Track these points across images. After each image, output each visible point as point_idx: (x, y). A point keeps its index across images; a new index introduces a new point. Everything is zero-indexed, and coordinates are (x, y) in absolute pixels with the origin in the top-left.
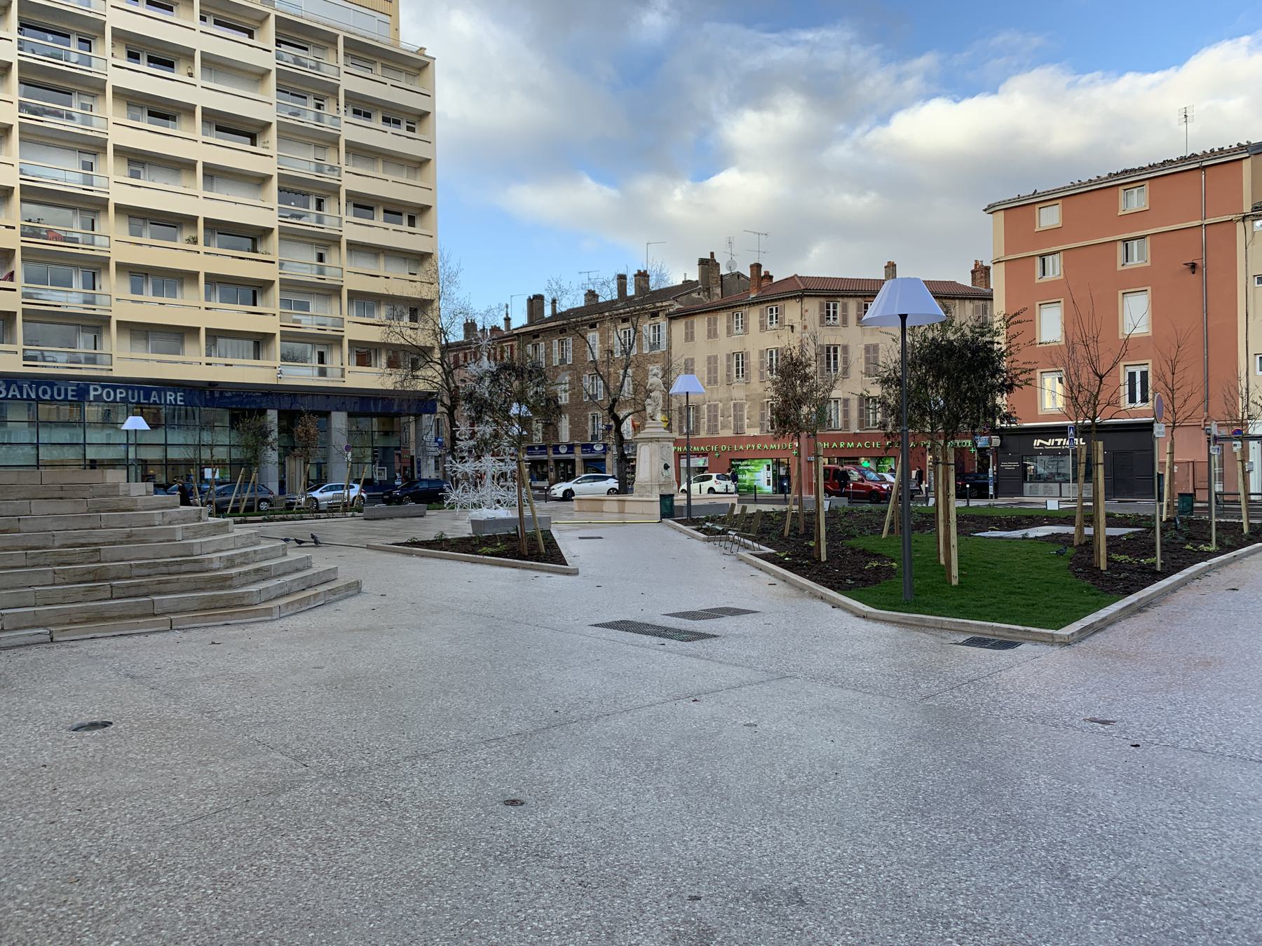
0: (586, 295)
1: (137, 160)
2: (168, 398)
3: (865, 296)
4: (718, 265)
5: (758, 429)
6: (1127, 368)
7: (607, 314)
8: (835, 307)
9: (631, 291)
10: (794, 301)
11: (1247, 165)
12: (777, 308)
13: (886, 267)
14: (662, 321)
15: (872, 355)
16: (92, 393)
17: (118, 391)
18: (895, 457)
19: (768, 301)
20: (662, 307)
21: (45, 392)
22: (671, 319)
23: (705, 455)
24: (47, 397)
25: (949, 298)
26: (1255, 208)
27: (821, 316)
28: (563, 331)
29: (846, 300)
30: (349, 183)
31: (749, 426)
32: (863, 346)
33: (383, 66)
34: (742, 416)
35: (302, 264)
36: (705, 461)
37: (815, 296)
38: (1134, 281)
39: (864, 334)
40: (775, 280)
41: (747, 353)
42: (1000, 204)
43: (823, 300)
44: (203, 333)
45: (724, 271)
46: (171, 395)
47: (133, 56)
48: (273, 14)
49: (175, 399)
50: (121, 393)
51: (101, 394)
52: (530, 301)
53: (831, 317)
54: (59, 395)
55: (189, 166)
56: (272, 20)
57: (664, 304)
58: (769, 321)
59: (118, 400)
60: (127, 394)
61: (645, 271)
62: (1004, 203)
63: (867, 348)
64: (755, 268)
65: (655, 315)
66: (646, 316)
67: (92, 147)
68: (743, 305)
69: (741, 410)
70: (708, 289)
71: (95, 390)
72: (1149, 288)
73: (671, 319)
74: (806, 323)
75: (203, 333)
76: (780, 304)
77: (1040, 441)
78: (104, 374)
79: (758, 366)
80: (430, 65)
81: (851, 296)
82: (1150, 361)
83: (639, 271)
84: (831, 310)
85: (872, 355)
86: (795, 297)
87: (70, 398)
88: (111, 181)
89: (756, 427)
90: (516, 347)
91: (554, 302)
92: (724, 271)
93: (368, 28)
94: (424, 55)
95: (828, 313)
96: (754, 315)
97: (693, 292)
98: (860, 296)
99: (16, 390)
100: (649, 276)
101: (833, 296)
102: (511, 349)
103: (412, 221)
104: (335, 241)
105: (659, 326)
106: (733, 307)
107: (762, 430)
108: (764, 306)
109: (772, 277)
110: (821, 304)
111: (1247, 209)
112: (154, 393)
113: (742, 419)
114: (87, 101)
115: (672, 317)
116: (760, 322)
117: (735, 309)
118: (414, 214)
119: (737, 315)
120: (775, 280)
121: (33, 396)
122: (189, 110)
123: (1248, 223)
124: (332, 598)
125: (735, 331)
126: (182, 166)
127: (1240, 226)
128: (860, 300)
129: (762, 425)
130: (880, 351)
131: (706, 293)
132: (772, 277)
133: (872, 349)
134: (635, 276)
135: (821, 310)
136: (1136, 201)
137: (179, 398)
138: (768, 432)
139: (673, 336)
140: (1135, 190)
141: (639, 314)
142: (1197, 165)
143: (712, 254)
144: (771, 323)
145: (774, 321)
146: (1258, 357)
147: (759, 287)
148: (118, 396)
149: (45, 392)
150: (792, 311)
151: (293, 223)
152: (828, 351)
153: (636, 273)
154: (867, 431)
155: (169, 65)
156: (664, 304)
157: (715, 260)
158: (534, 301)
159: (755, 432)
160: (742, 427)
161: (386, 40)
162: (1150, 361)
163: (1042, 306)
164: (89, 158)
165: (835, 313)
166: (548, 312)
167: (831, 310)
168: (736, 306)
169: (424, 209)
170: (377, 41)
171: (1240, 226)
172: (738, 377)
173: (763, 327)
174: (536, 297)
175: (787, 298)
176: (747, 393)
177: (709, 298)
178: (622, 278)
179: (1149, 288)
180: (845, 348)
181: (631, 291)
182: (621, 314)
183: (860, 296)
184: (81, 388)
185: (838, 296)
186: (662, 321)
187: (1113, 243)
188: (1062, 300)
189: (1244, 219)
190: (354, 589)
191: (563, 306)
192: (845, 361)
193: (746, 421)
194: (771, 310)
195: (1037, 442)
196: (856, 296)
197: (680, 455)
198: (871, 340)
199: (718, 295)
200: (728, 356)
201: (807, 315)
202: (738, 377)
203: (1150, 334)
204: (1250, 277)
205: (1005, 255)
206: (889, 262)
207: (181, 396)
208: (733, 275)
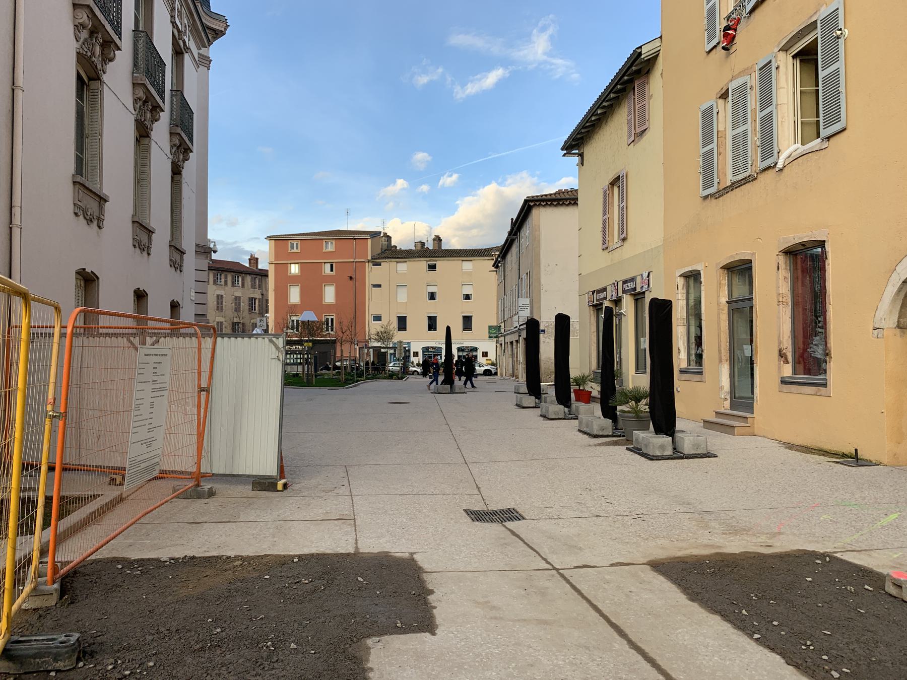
11: (369, 241)
38: (329, 280)
82: (334, 314)
111: (369, 258)
136: (330, 247)
140: (330, 242)
142: (352, 238)
162: (334, 314)
171: (367, 263)
203: (335, 303)
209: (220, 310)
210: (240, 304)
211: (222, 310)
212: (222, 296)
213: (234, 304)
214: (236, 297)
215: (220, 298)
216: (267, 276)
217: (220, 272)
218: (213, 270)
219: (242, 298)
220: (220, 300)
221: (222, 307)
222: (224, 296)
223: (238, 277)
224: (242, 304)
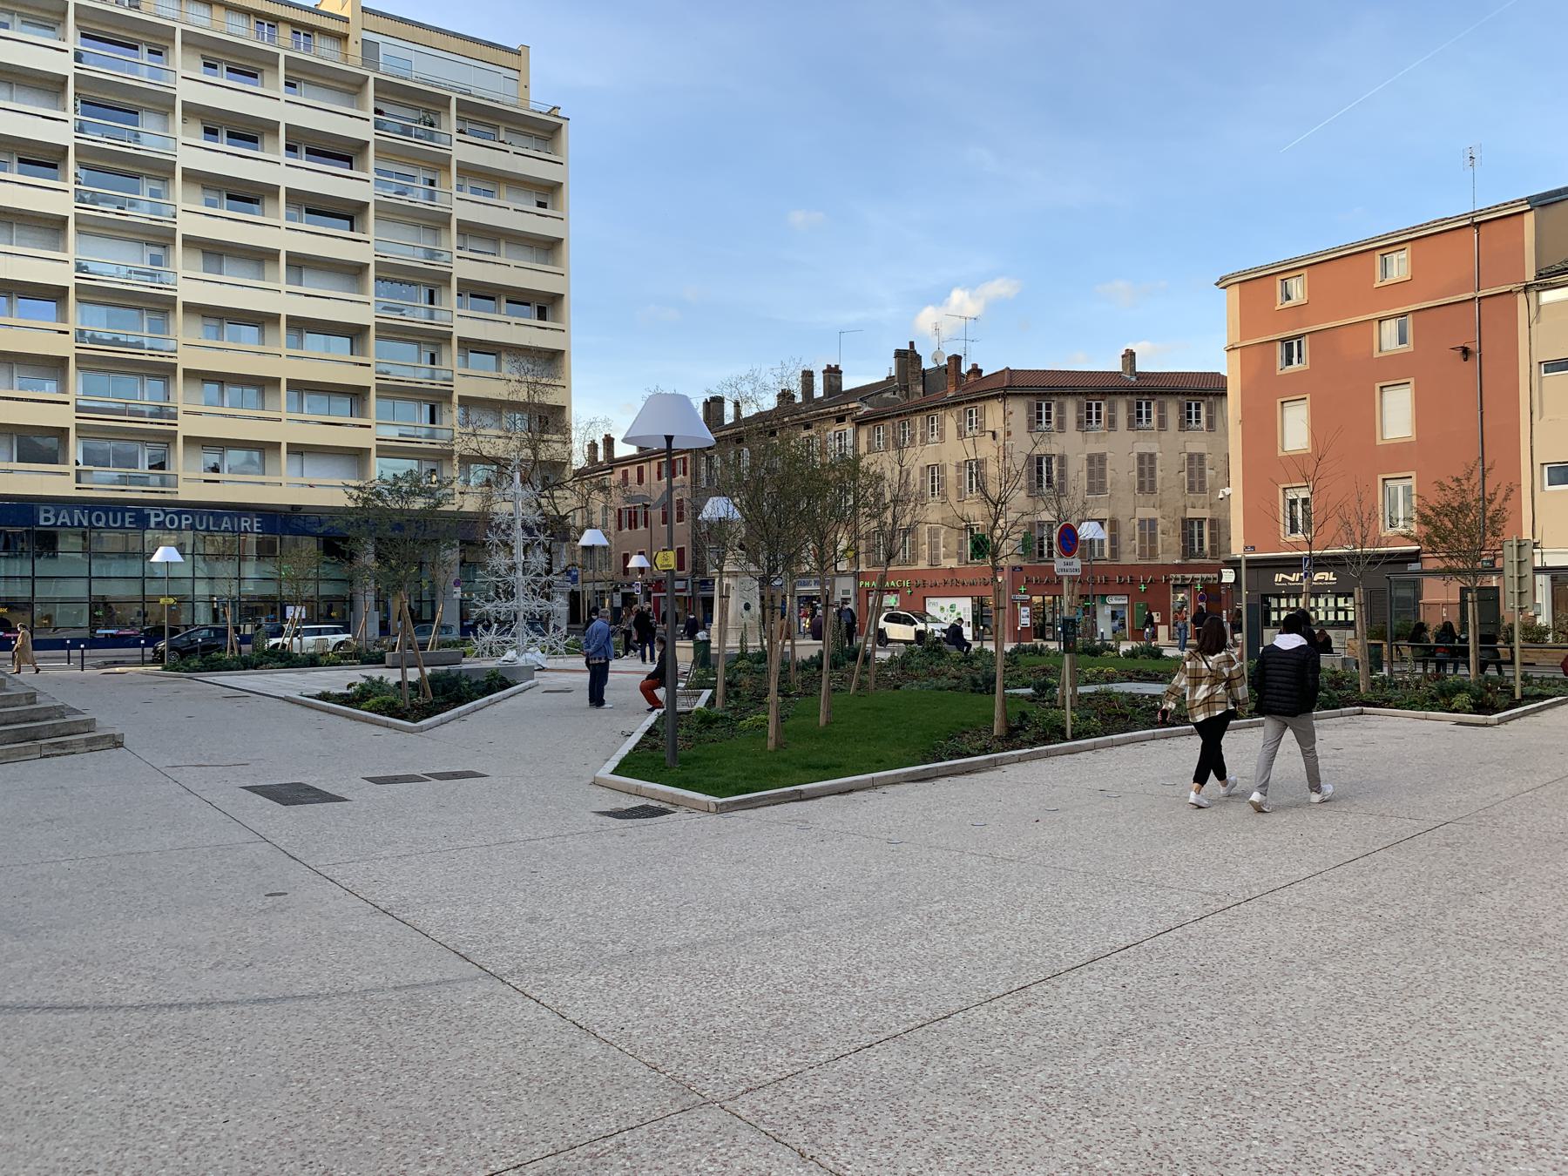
0: (779, 396)
1: (214, 252)
2: (243, 524)
4: (919, 358)
5: (956, 560)
6: (1387, 482)
7: (786, 419)
8: (1048, 407)
9: (819, 392)
11: (1529, 219)
13: (1123, 356)
14: (848, 427)
15: (1096, 467)
16: (153, 520)
17: (184, 517)
18: (1128, 595)
19: (968, 402)
20: (848, 409)
21: (99, 519)
22: (858, 424)
23: (896, 591)
24: (101, 524)
25: (1200, 394)
26: (1539, 275)
28: (739, 441)
29: (1062, 399)
30: (465, 269)
31: (946, 556)
32: (1085, 457)
33: (507, 130)
34: (938, 543)
35: (408, 365)
37: (1022, 394)
38: (1392, 371)
39: (1086, 442)
40: (984, 375)
41: (942, 466)
42: (1233, 276)
43: (1033, 400)
44: (284, 448)
45: (927, 364)
46: (246, 522)
47: (211, 132)
48: (372, 76)
49: (251, 526)
50: (187, 519)
51: (164, 521)
52: (706, 404)
54: (115, 522)
55: (269, 256)
56: (371, 82)
57: (851, 406)
58: (968, 426)
59: (183, 527)
60: (194, 520)
61: (837, 366)
62: (1239, 274)
63: (1090, 459)
64: (953, 361)
65: (841, 420)
67: (160, 238)
68: (937, 407)
69: (937, 535)
71: (157, 516)
72: (1412, 380)
73: (858, 424)
74: (1010, 428)
75: (284, 448)
76: (979, 405)
77: (1282, 576)
78: (168, 497)
79: (955, 481)
80: (564, 127)
81: (1069, 394)
82: (1413, 474)
83: (829, 366)
84: (1044, 411)
86: (997, 396)
87: (127, 525)
88: (179, 276)
89: (953, 557)
90: (689, 461)
91: (737, 405)
92: (927, 364)
93: (489, 87)
94: (558, 117)
95: (1039, 415)
96: (950, 421)
97: (885, 391)
98: (1080, 394)
99: (67, 516)
100: (841, 372)
101: (1045, 394)
102: (685, 463)
103: (542, 315)
104: (447, 337)
106: (927, 409)
107: (960, 561)
108: (961, 408)
109: (981, 371)
111: (1530, 276)
112: (226, 519)
113: (937, 548)
114: (157, 186)
115: (860, 423)
116: (958, 427)
118: (546, 305)
119: (933, 419)
120: (984, 375)
121: (86, 523)
122: (273, 191)
123: (1532, 295)
124: (58, 752)
125: (930, 439)
126: (261, 257)
127: (1521, 297)
128: (1081, 398)
129: (960, 555)
131: (904, 392)
132: (981, 371)
133: (1146, 459)
134: (824, 372)
135: (1030, 412)
137: (255, 525)
138: (967, 563)
141: (823, 418)
142: (1468, 222)
143: (912, 344)
145: (974, 425)
146: (1546, 467)
147: (957, 386)
148: (184, 522)
149: (99, 519)
150: (994, 414)
151: (393, 318)
153: (825, 368)
154: (1043, 564)
155: (252, 140)
156: (851, 406)
157: (915, 352)
159: (952, 563)
160: (937, 557)
161: (509, 100)
162: (1413, 474)
163: (1285, 405)
164: (157, 251)
166: (729, 418)
168: (931, 408)
169: (556, 299)
170: (497, 102)
171: (1521, 297)
172: (971, 491)
173: (961, 434)
174: (713, 399)
175: (989, 398)
176: (944, 516)
177: (908, 397)
178: (808, 376)
179: (1412, 380)
180: (1062, 460)
181: (819, 392)
182: (802, 419)
183: (1080, 394)
184: (136, 515)
186: (848, 427)
187: (1368, 323)
188: (1308, 396)
189: (1526, 289)
190: (117, 742)
191: (748, 411)
192: (1062, 474)
193: (943, 549)
195: (1279, 577)
197: (868, 592)
199: (919, 394)
200: (922, 469)
202: (933, 495)
204: (1535, 365)
207: (258, 522)
208: (939, 369)
209: (1147, 489)
210: (1202, 473)
211: (1153, 490)
212: (1152, 456)
213: (1185, 474)
214: (1191, 456)
215: (1146, 463)
216: (1222, 394)
217: (1147, 397)
218: (1127, 393)
220: (1146, 467)
221: (1152, 483)
222: (1158, 455)
223: (1148, 406)
224: (1208, 472)
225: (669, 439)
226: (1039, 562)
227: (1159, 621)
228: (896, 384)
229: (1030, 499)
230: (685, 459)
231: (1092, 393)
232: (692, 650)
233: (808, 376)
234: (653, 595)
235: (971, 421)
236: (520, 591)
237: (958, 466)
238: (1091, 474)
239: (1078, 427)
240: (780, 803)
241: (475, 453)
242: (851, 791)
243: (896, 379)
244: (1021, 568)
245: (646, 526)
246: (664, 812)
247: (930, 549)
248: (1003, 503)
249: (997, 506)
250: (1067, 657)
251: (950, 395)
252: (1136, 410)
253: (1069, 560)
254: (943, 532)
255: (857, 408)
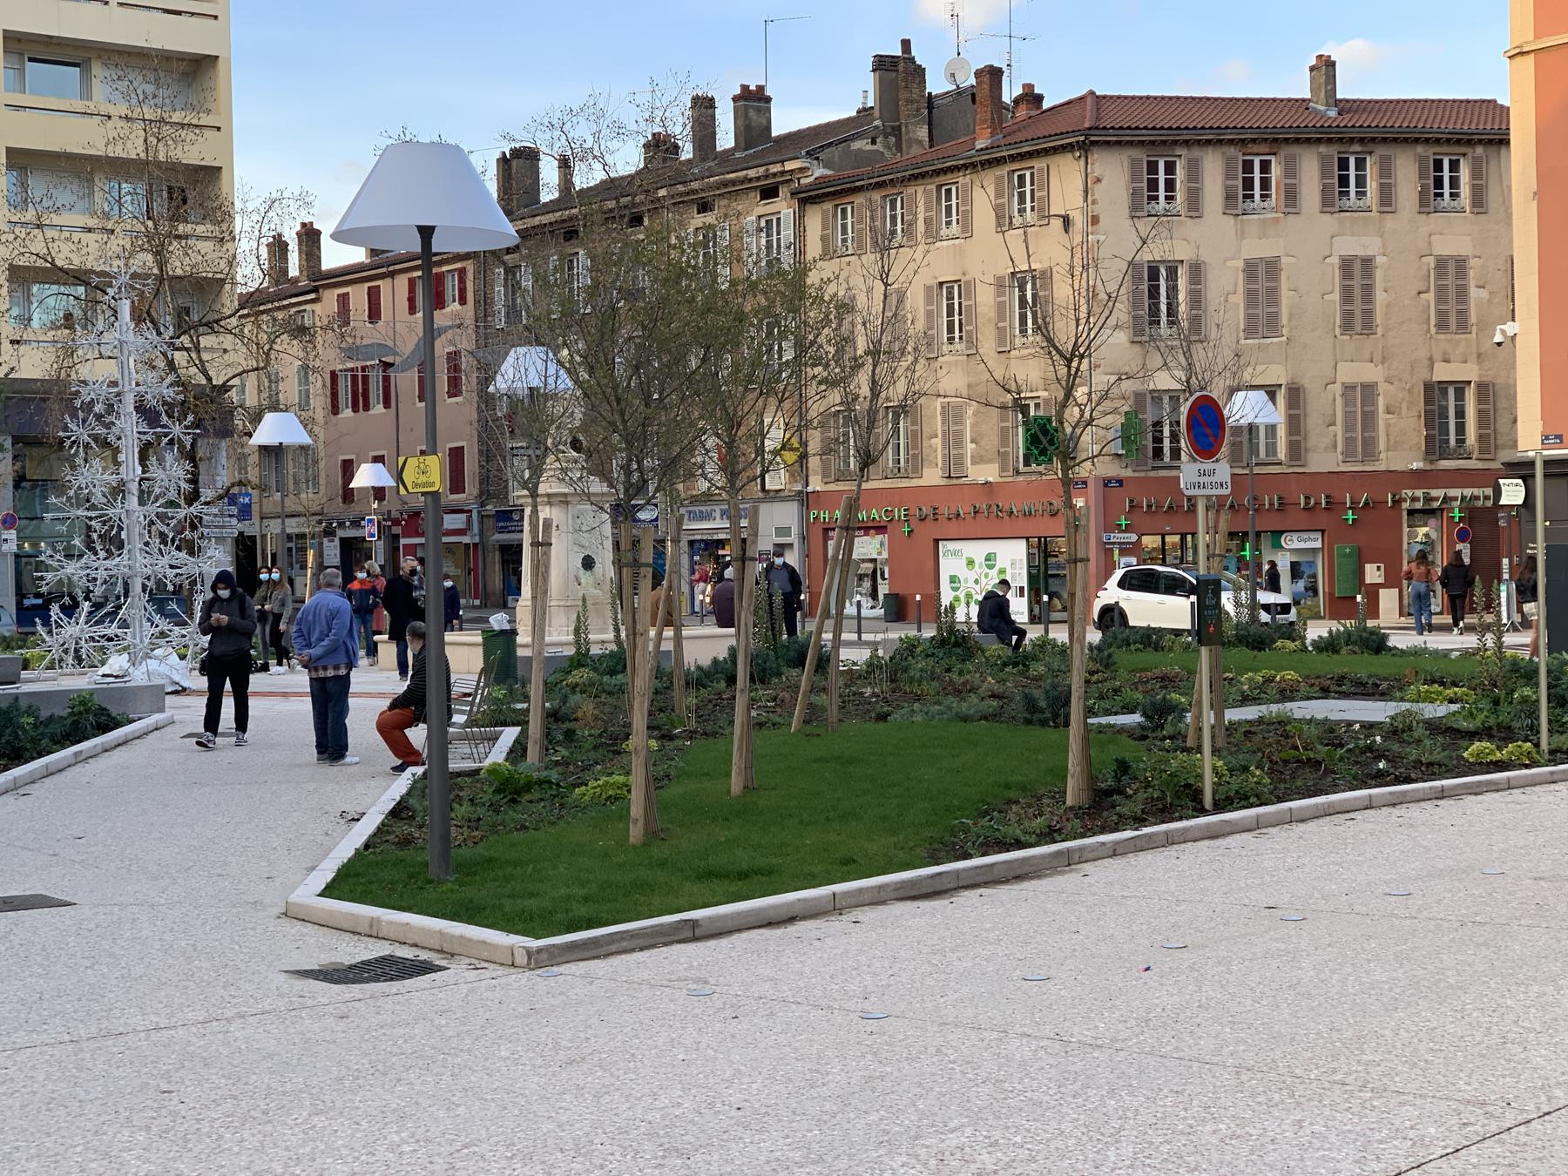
0: (647, 146)
3: (1243, 141)
4: (920, 72)
7: (662, 192)
8: (1170, 168)
9: (726, 139)
10: (1070, 155)
12: (1032, 174)
13: (1312, 69)
14: (784, 207)
15: (1261, 285)
18: (1323, 531)
19: (1013, 158)
20: (783, 173)
23: (881, 529)
25: (1458, 142)
27: (1135, 194)
28: (571, 235)
29: (1196, 152)
32: (1241, 264)
36: (882, 544)
37: (1119, 143)
39: (1241, 235)
40: (1046, 105)
43: (1142, 155)
45: (936, 84)
52: (504, 161)
53: (1162, 193)
57: (789, 166)
58: (1016, 207)
61: (761, 88)
63: (1251, 269)
64: (986, 79)
65: (769, 193)
66: (752, 194)
68: (957, 168)
70: (897, 131)
74: (1097, 209)
76: (1039, 164)
79: (992, 313)
81: (1209, 142)
83: (745, 88)
84: (1162, 177)
85: (1261, 285)
89: (990, 461)
91: (565, 164)
92: (936, 84)
95: (1153, 185)
96: (982, 194)
98: (1231, 142)
100: (768, 100)
101: (1164, 142)
102: (462, 281)
105: (779, 220)
106: (938, 173)
107: (1003, 469)
108: (1003, 171)
110: (1134, 163)
113: (959, 443)
115: (807, 198)
117: (942, 179)
119: (949, 192)
120: (1046, 105)
125: (944, 232)
128: (1232, 151)
129: (1002, 457)
130: (1284, 275)
131: (892, 140)
133: (1357, 266)
134: (735, 99)
135: (1135, 177)
138: (1018, 473)
139: (808, 243)
143: (906, 44)
144: (1022, 211)
145: (1028, 205)
147: (996, 124)
152: (1154, 274)
153: (738, 92)
156: (789, 166)
157: (912, 60)
158: (514, 163)
159: (988, 473)
160: (960, 461)
165: (1170, 186)
167: (1162, 177)
168: (945, 171)
172: (1023, 331)
173: (1003, 222)
174: (517, 153)
175: (1055, 150)
176: (972, 380)
177: (899, 148)
178: (704, 106)
180: (1197, 271)
181: (726, 139)
182: (694, 192)
183: (1231, 142)
185: (1175, 142)
186: (784, 207)
191: (586, 177)
192: (1196, 300)
193: (970, 447)
194: (1021, 178)
196: (1220, 142)
197: (826, 530)
198: (1352, 246)
199: (920, 142)
200: (928, 289)
201: (1099, 191)
202: (951, 340)
205: (1537, 37)
206: (1320, 57)
208: (959, 93)
209: (1358, 328)
210: (1462, 293)
211: (1368, 327)
212: (1367, 263)
213: (1430, 297)
214: (1441, 263)
216: (1501, 141)
217: (1357, 148)
218: (1319, 141)
219: (1472, 262)
220: (1357, 283)
221: (1368, 315)
222: (1380, 260)
223: (1360, 164)
224: (1474, 293)
225: (426, 232)
226: (1154, 468)
227: (1381, 580)
228: (877, 123)
229: (1137, 348)
230: (462, 272)
231: (1254, 141)
232: (480, 650)
233: (704, 106)
234: (403, 541)
235: (1022, 197)
236: (134, 535)
237: (999, 284)
238: (1251, 298)
239: (1227, 207)
240: (654, 946)
241: (40, 263)
242: (792, 920)
243: (877, 113)
244: (1120, 482)
245: (387, 404)
246: (425, 968)
247: (947, 444)
248: (1082, 357)
249: (1069, 361)
250: (1204, 651)
251: (980, 144)
252: (1337, 173)
253: (1207, 465)
254: (970, 412)
255: (802, 170)
